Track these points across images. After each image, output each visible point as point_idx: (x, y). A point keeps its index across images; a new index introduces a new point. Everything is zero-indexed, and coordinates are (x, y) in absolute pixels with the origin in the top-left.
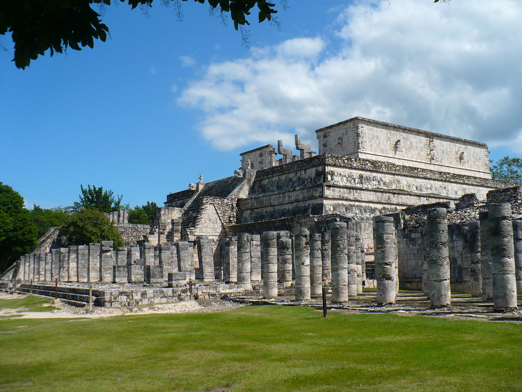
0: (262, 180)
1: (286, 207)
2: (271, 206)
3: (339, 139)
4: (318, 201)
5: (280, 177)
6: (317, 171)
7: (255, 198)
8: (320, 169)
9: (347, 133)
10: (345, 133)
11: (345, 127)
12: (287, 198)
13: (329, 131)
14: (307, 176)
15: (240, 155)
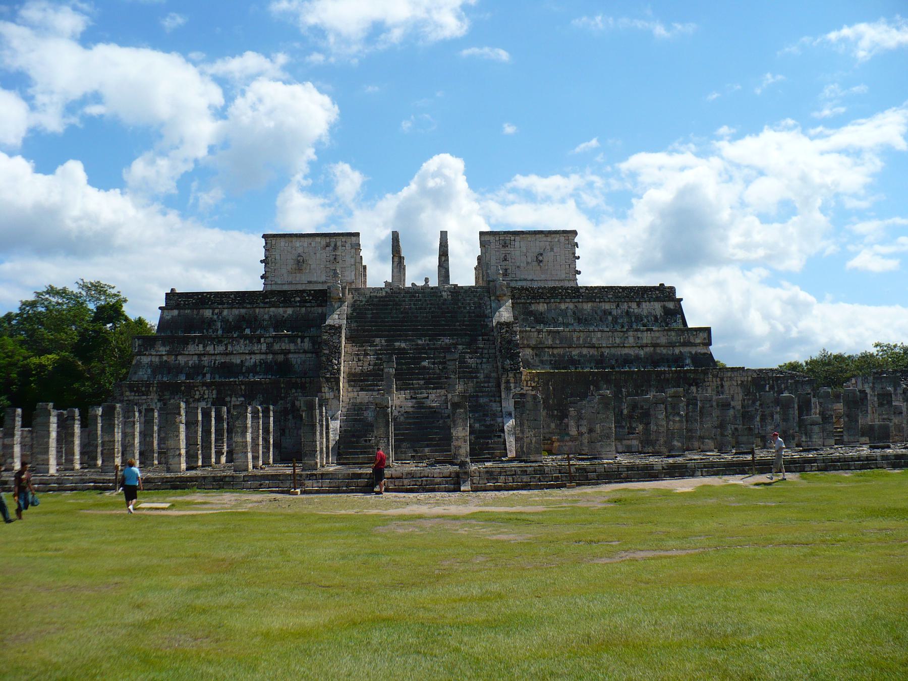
0: (530, 303)
1: (631, 352)
2: (593, 347)
3: (541, 254)
4: (701, 350)
5: (580, 305)
6: (664, 307)
7: (549, 332)
8: (671, 305)
9: (552, 249)
10: (548, 247)
11: (549, 239)
12: (631, 340)
13: (512, 238)
14: (645, 313)
15: (264, 236)
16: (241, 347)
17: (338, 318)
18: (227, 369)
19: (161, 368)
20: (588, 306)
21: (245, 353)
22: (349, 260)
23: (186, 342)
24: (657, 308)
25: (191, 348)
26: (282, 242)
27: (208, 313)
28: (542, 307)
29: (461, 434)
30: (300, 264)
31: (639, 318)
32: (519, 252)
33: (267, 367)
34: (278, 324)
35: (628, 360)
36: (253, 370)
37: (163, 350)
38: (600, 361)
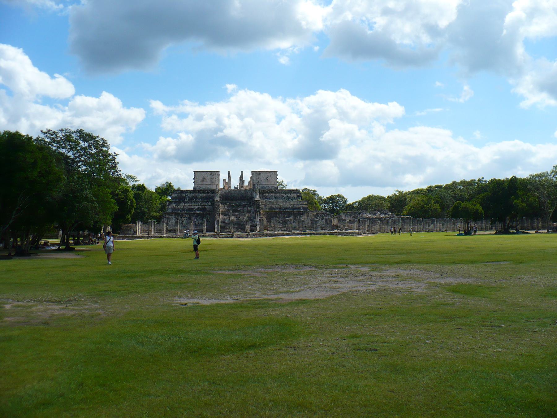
16: (194, 204)
17: (217, 198)
18: (190, 209)
19: (174, 209)
20: (278, 195)
21: (195, 206)
22: (217, 178)
23: (180, 203)
24: (295, 195)
25: (181, 204)
26: (199, 173)
27: (184, 195)
28: (267, 195)
29: (248, 227)
30: (204, 179)
31: (290, 198)
32: (262, 177)
33: (200, 209)
34: (202, 198)
35: (287, 208)
36: (197, 210)
37: (174, 205)
38: (280, 209)
